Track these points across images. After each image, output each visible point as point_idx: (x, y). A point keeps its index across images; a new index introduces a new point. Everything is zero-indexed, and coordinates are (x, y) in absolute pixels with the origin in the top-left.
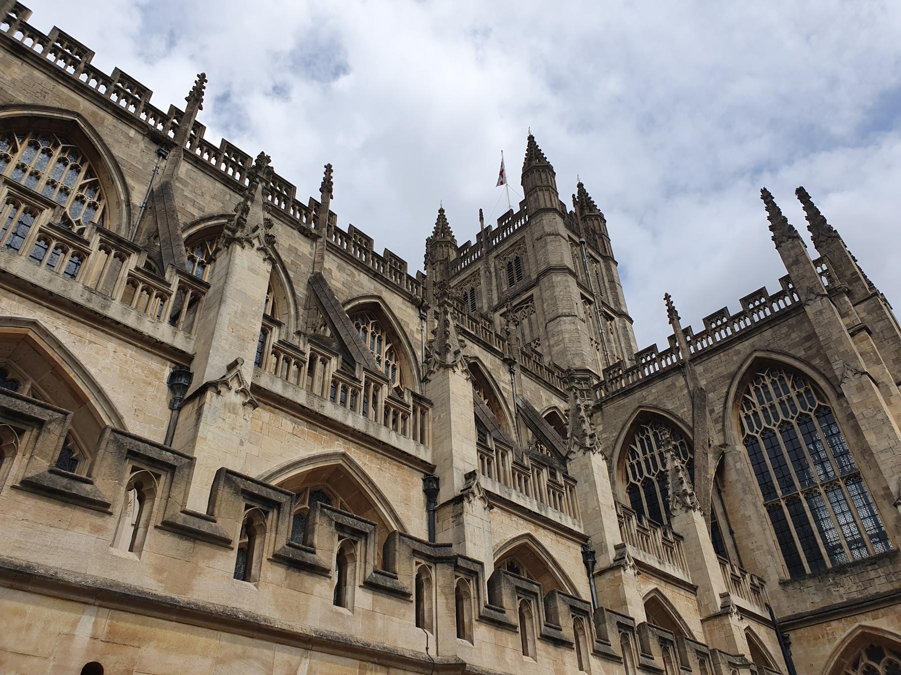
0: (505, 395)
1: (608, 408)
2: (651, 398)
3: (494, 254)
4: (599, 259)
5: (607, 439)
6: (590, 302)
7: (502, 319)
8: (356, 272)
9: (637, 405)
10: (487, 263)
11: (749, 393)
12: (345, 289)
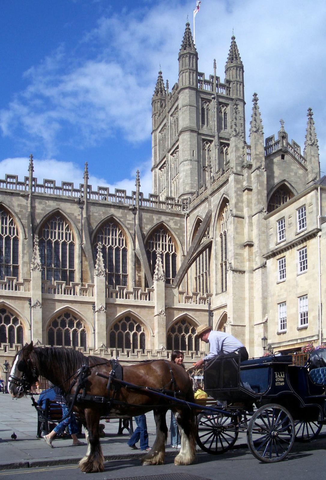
0: (129, 226)
1: (191, 215)
2: (200, 212)
3: (170, 113)
4: (229, 102)
5: (189, 230)
6: (211, 141)
7: (171, 156)
8: (47, 202)
9: (197, 215)
10: (168, 120)
11: (223, 213)
12: (43, 212)
